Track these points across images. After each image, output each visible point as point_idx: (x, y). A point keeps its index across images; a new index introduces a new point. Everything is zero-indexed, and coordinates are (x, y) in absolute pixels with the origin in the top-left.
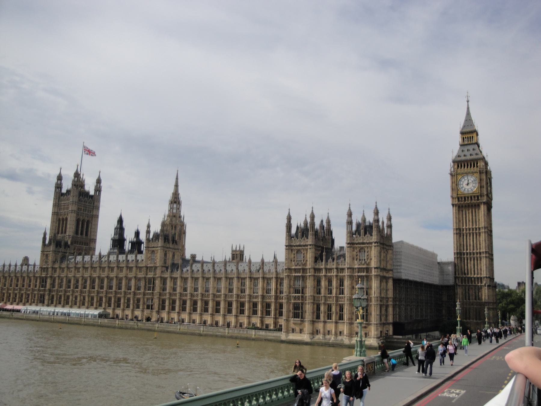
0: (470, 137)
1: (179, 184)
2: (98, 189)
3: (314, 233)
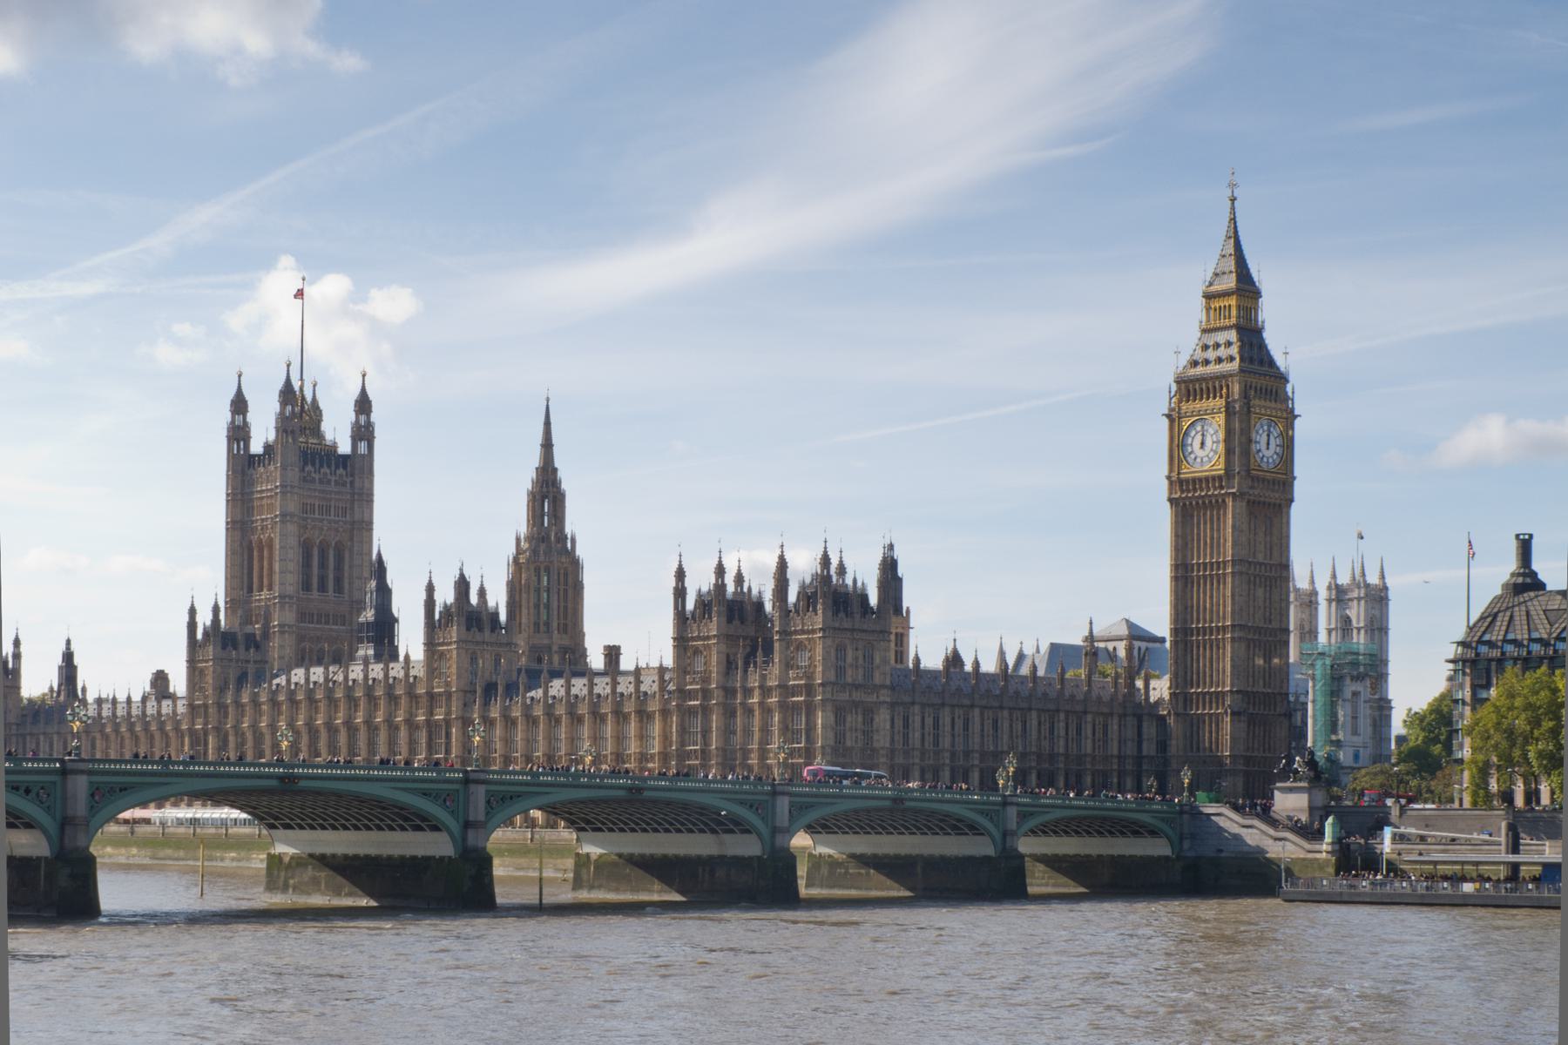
0: (1220, 307)
1: (554, 442)
2: (363, 432)
3: (723, 609)
